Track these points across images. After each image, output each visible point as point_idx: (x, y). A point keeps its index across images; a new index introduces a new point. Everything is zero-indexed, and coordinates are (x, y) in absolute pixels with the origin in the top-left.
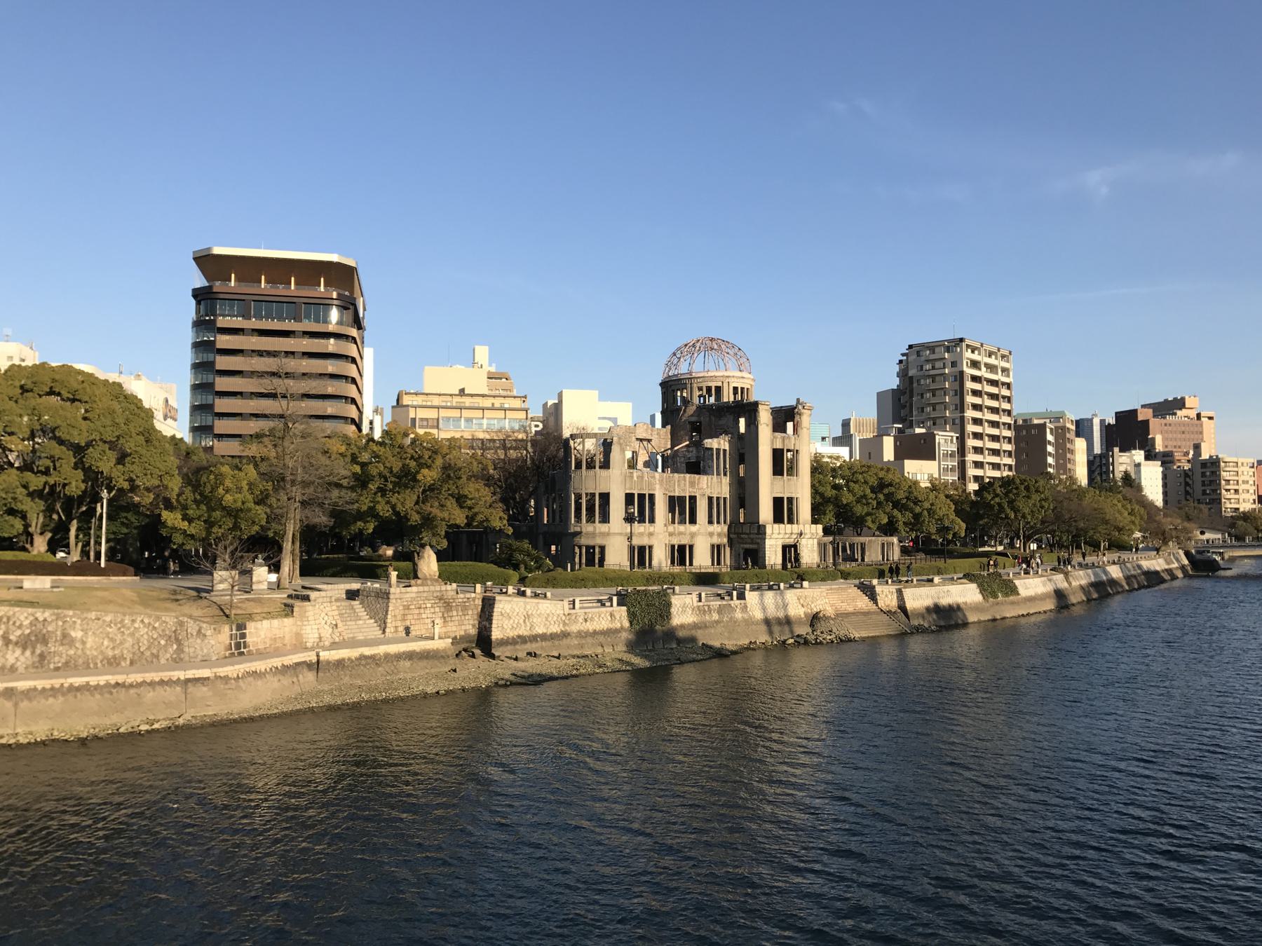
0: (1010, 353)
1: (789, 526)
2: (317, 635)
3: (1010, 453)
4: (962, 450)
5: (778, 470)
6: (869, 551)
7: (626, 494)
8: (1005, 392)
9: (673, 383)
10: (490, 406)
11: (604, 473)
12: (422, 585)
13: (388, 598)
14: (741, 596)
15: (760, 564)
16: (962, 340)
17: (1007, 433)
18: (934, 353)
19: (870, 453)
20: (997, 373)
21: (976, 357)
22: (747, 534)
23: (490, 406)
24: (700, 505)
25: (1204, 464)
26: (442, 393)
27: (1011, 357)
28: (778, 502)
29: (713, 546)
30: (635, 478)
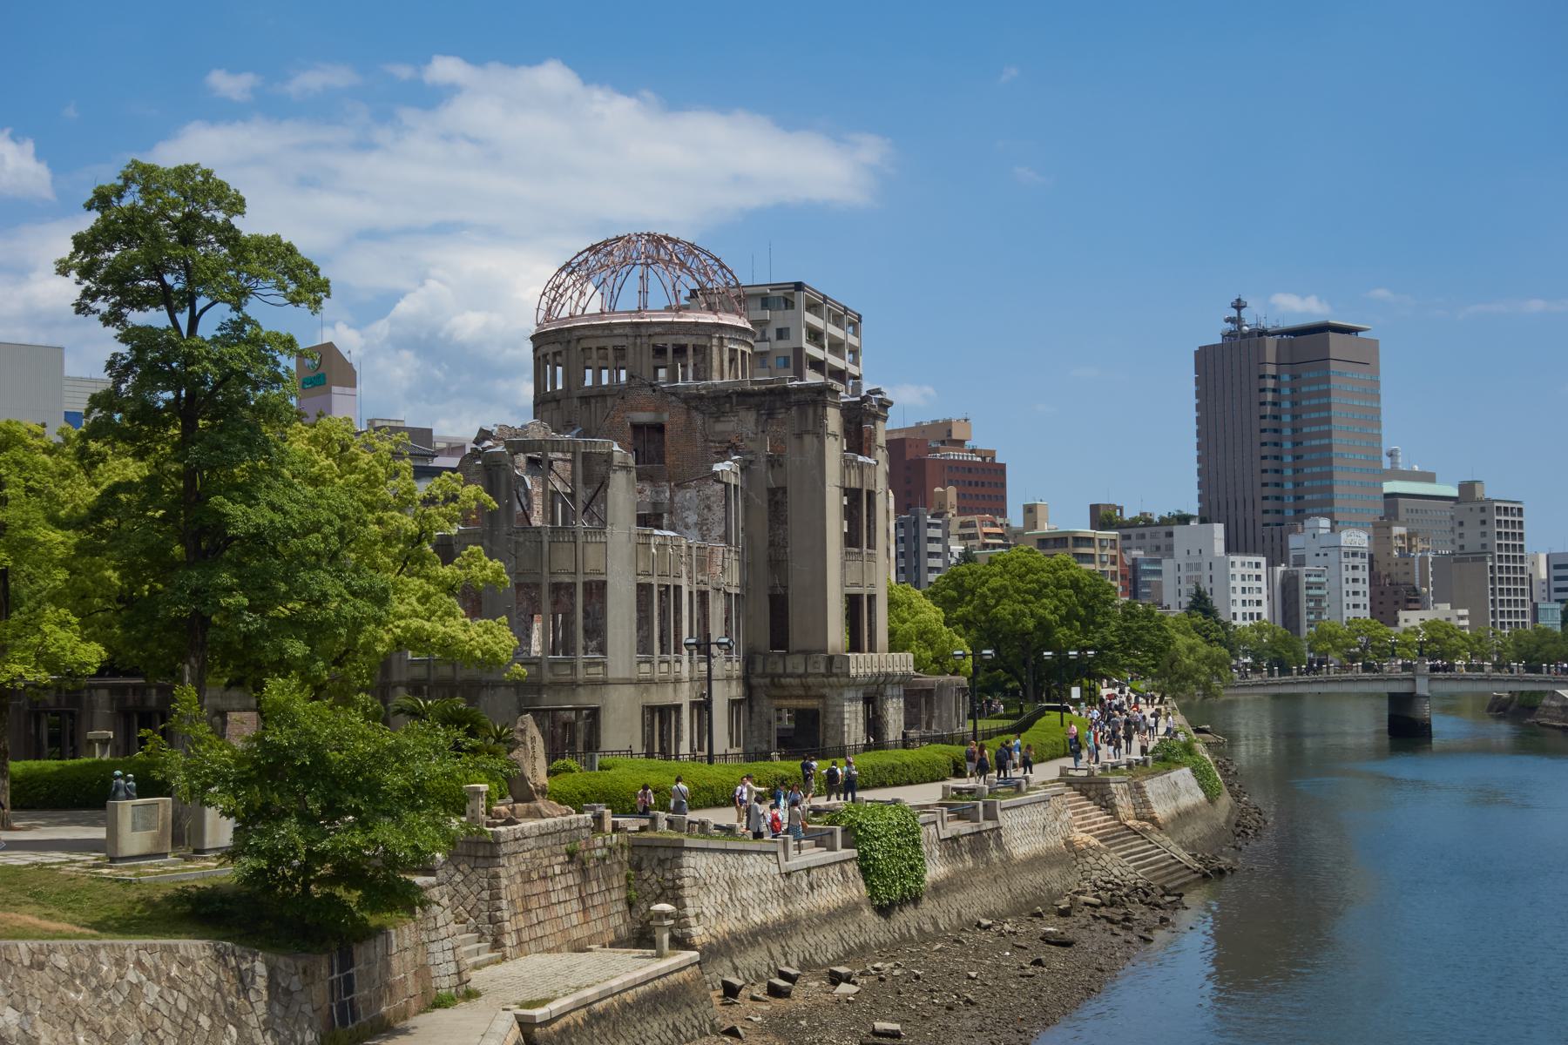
0: (860, 321)
5: (851, 540)
6: (939, 707)
9: (587, 333)
15: (830, 744)
16: (799, 286)
20: (844, 359)
22: (800, 676)
24: (714, 614)
25: (1043, 542)
27: (863, 326)
30: (654, 550)
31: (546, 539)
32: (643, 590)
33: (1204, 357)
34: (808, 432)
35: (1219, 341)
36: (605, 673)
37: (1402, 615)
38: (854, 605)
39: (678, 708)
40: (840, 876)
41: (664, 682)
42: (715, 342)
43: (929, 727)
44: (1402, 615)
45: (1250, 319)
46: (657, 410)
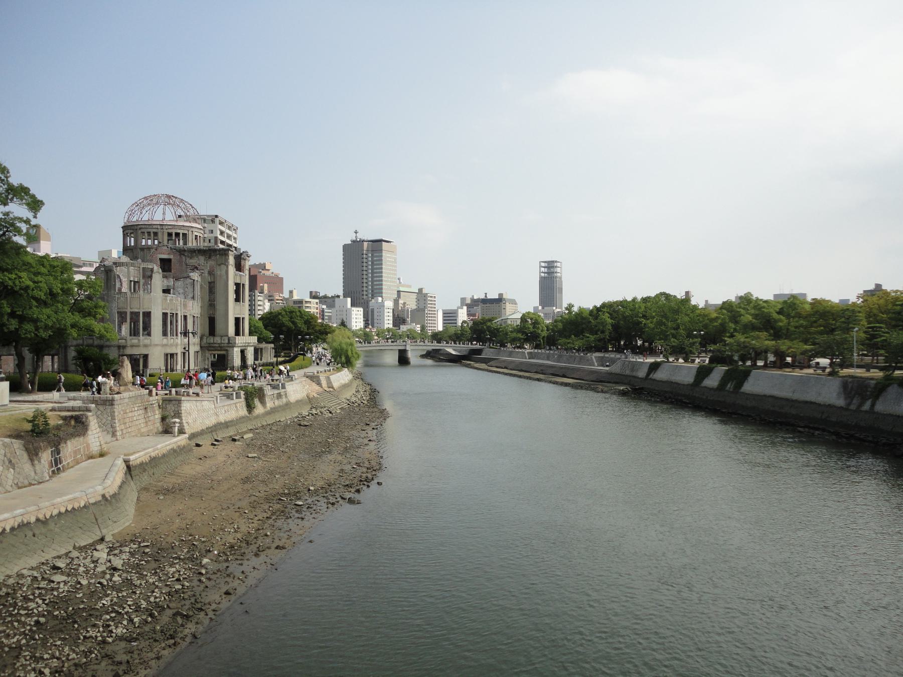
1: (242, 337)
2: (98, 444)
5: (237, 300)
7: (163, 313)
9: (141, 226)
11: (147, 296)
12: (125, 391)
13: (112, 405)
16: (216, 216)
21: (223, 229)
25: (295, 302)
27: (238, 231)
29: (195, 352)
31: (128, 296)
32: (165, 315)
33: (346, 247)
34: (222, 264)
35: (350, 243)
36: (151, 342)
37: (401, 326)
38: (237, 320)
39: (177, 354)
41: (172, 345)
42: (190, 232)
43: (261, 360)
44: (401, 326)
45: (361, 236)
46: (169, 254)
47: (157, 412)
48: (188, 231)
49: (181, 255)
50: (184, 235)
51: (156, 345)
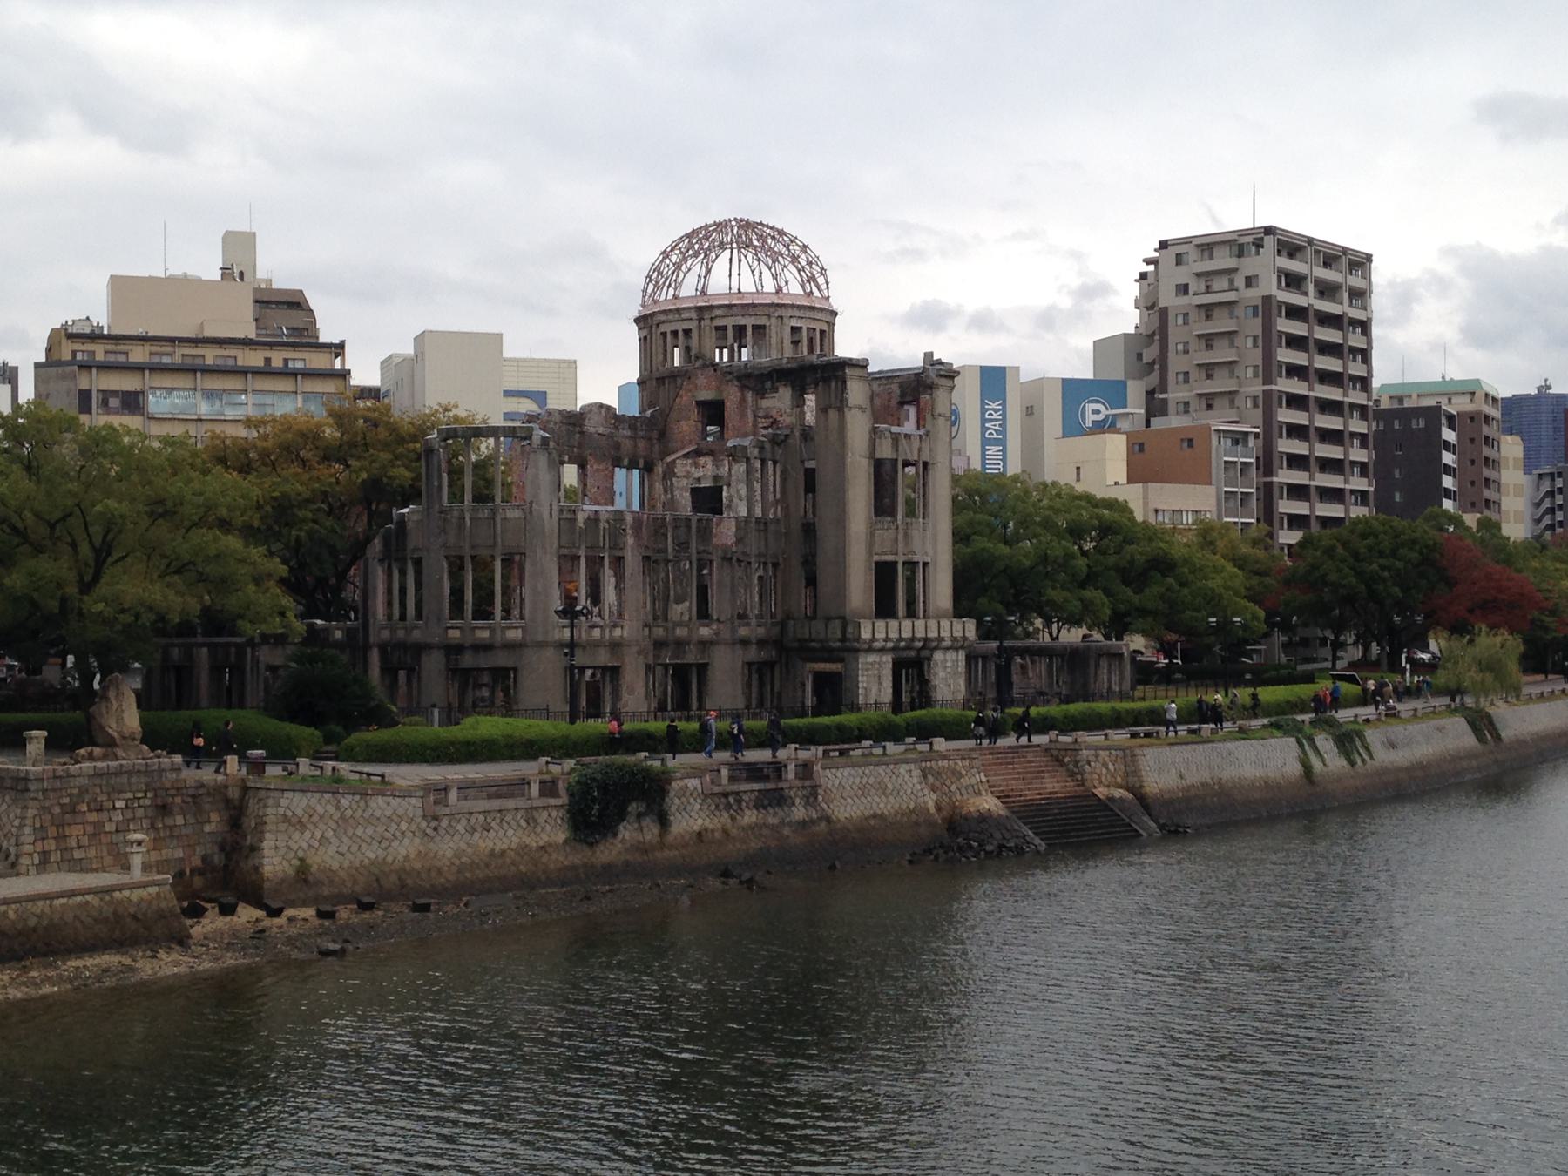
3: (1363, 466)
4: (1266, 464)
5: (883, 504)
8: (1356, 340)
9: (663, 317)
10: (261, 364)
12: (104, 757)
14: (806, 769)
16: (1269, 230)
17: (1358, 426)
18: (1211, 258)
19: (1078, 468)
22: (821, 641)
23: (261, 364)
26: (154, 332)
28: (884, 574)
40: (523, 823)
42: (773, 320)
47: (214, 817)
48: (769, 316)
49: (743, 388)
50: (759, 330)
51: (542, 645)
